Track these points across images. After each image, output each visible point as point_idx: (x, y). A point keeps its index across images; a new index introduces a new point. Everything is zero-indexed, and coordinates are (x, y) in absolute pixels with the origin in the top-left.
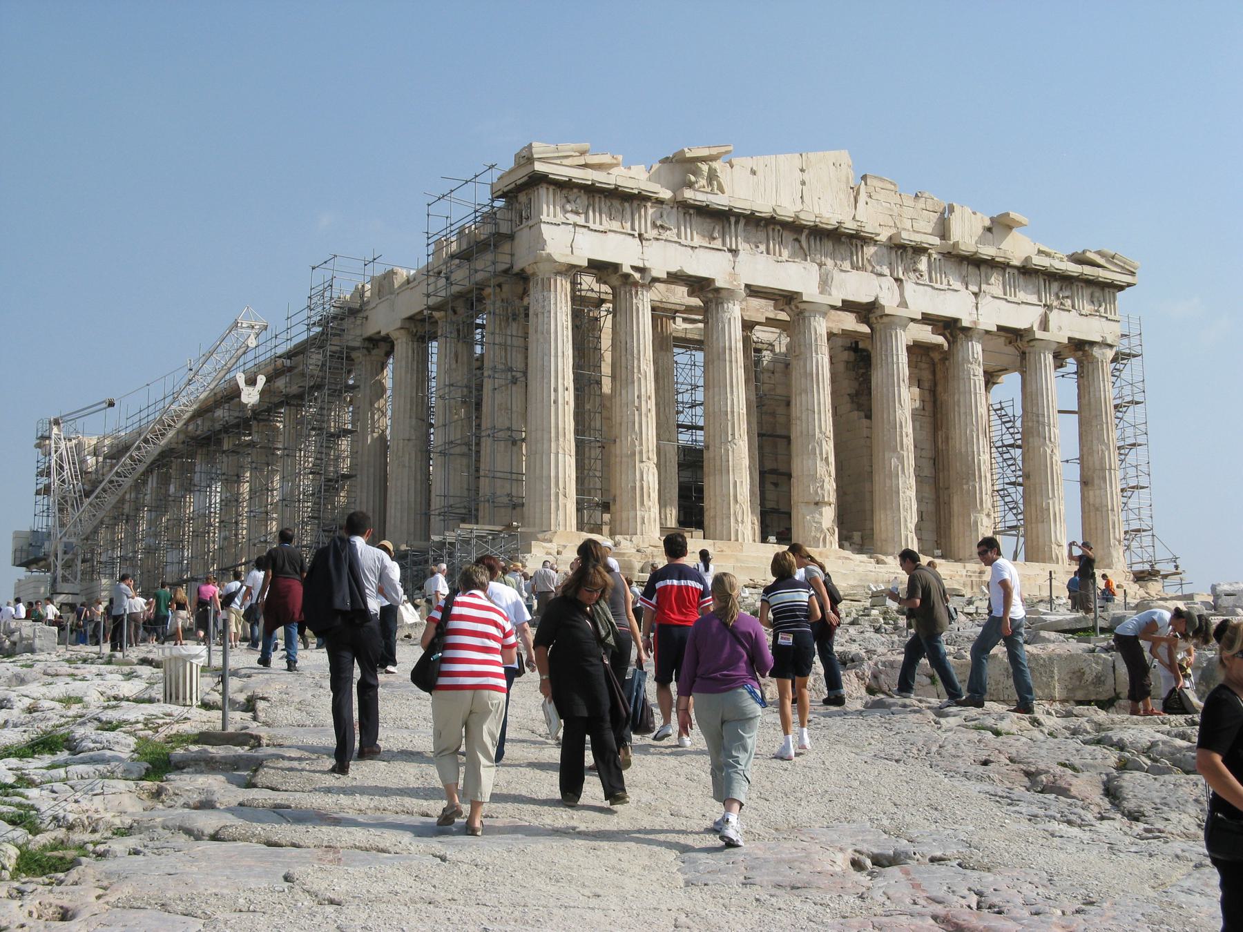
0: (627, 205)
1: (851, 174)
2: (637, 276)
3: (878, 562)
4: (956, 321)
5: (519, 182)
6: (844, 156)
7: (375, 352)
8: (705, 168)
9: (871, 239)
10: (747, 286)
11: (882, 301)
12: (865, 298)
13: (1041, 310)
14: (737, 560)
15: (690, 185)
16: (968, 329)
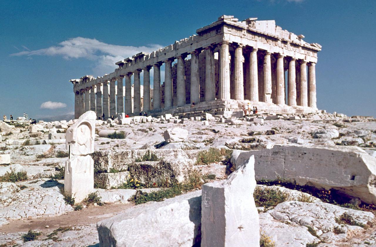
2: (240, 45)
6: (274, 21)
8: (252, 22)
10: (258, 49)
11: (280, 53)
12: (277, 52)
13: (305, 55)
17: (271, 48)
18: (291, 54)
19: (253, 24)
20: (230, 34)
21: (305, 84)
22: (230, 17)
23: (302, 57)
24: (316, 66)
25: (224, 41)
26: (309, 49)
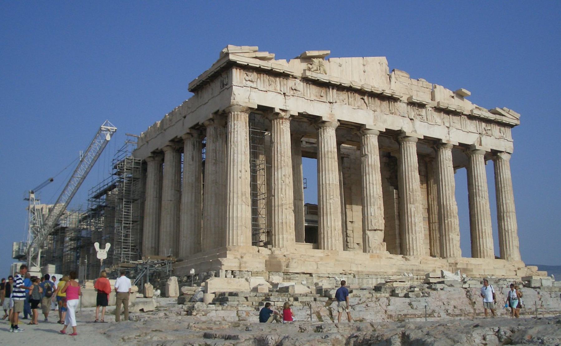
0: (278, 79)
1: (388, 68)
2: (283, 114)
3: (406, 259)
4: (440, 140)
5: (222, 66)
7: (157, 159)
8: (314, 60)
9: (399, 99)
10: (339, 121)
11: (405, 130)
12: (396, 128)
13: (478, 136)
14: (336, 260)
15: (309, 69)
16: (445, 144)
17: (374, 119)
18: (436, 133)
19: (320, 65)
20: (251, 87)
21: (484, 203)
22: (246, 48)
23: (469, 140)
24: (511, 161)
25: (233, 105)
26: (487, 121)
